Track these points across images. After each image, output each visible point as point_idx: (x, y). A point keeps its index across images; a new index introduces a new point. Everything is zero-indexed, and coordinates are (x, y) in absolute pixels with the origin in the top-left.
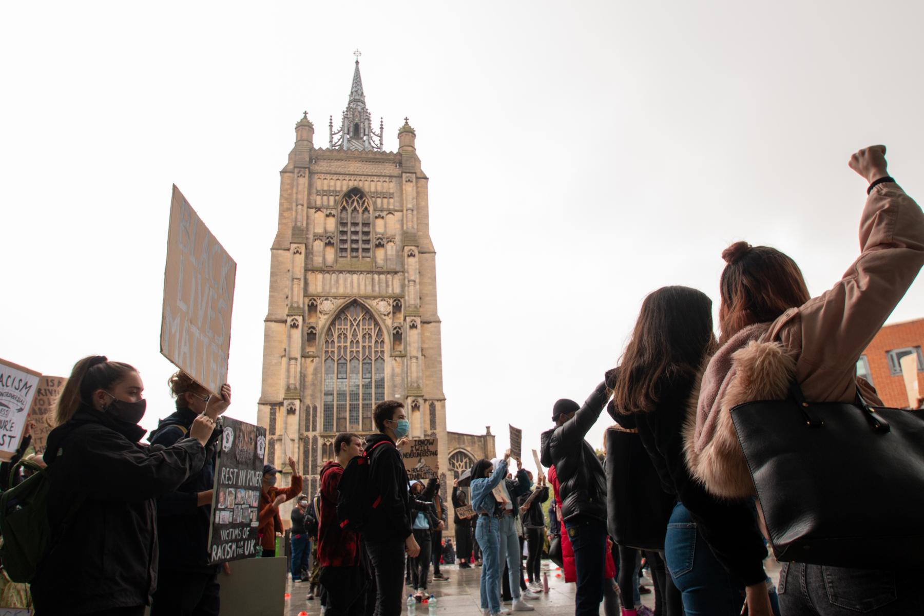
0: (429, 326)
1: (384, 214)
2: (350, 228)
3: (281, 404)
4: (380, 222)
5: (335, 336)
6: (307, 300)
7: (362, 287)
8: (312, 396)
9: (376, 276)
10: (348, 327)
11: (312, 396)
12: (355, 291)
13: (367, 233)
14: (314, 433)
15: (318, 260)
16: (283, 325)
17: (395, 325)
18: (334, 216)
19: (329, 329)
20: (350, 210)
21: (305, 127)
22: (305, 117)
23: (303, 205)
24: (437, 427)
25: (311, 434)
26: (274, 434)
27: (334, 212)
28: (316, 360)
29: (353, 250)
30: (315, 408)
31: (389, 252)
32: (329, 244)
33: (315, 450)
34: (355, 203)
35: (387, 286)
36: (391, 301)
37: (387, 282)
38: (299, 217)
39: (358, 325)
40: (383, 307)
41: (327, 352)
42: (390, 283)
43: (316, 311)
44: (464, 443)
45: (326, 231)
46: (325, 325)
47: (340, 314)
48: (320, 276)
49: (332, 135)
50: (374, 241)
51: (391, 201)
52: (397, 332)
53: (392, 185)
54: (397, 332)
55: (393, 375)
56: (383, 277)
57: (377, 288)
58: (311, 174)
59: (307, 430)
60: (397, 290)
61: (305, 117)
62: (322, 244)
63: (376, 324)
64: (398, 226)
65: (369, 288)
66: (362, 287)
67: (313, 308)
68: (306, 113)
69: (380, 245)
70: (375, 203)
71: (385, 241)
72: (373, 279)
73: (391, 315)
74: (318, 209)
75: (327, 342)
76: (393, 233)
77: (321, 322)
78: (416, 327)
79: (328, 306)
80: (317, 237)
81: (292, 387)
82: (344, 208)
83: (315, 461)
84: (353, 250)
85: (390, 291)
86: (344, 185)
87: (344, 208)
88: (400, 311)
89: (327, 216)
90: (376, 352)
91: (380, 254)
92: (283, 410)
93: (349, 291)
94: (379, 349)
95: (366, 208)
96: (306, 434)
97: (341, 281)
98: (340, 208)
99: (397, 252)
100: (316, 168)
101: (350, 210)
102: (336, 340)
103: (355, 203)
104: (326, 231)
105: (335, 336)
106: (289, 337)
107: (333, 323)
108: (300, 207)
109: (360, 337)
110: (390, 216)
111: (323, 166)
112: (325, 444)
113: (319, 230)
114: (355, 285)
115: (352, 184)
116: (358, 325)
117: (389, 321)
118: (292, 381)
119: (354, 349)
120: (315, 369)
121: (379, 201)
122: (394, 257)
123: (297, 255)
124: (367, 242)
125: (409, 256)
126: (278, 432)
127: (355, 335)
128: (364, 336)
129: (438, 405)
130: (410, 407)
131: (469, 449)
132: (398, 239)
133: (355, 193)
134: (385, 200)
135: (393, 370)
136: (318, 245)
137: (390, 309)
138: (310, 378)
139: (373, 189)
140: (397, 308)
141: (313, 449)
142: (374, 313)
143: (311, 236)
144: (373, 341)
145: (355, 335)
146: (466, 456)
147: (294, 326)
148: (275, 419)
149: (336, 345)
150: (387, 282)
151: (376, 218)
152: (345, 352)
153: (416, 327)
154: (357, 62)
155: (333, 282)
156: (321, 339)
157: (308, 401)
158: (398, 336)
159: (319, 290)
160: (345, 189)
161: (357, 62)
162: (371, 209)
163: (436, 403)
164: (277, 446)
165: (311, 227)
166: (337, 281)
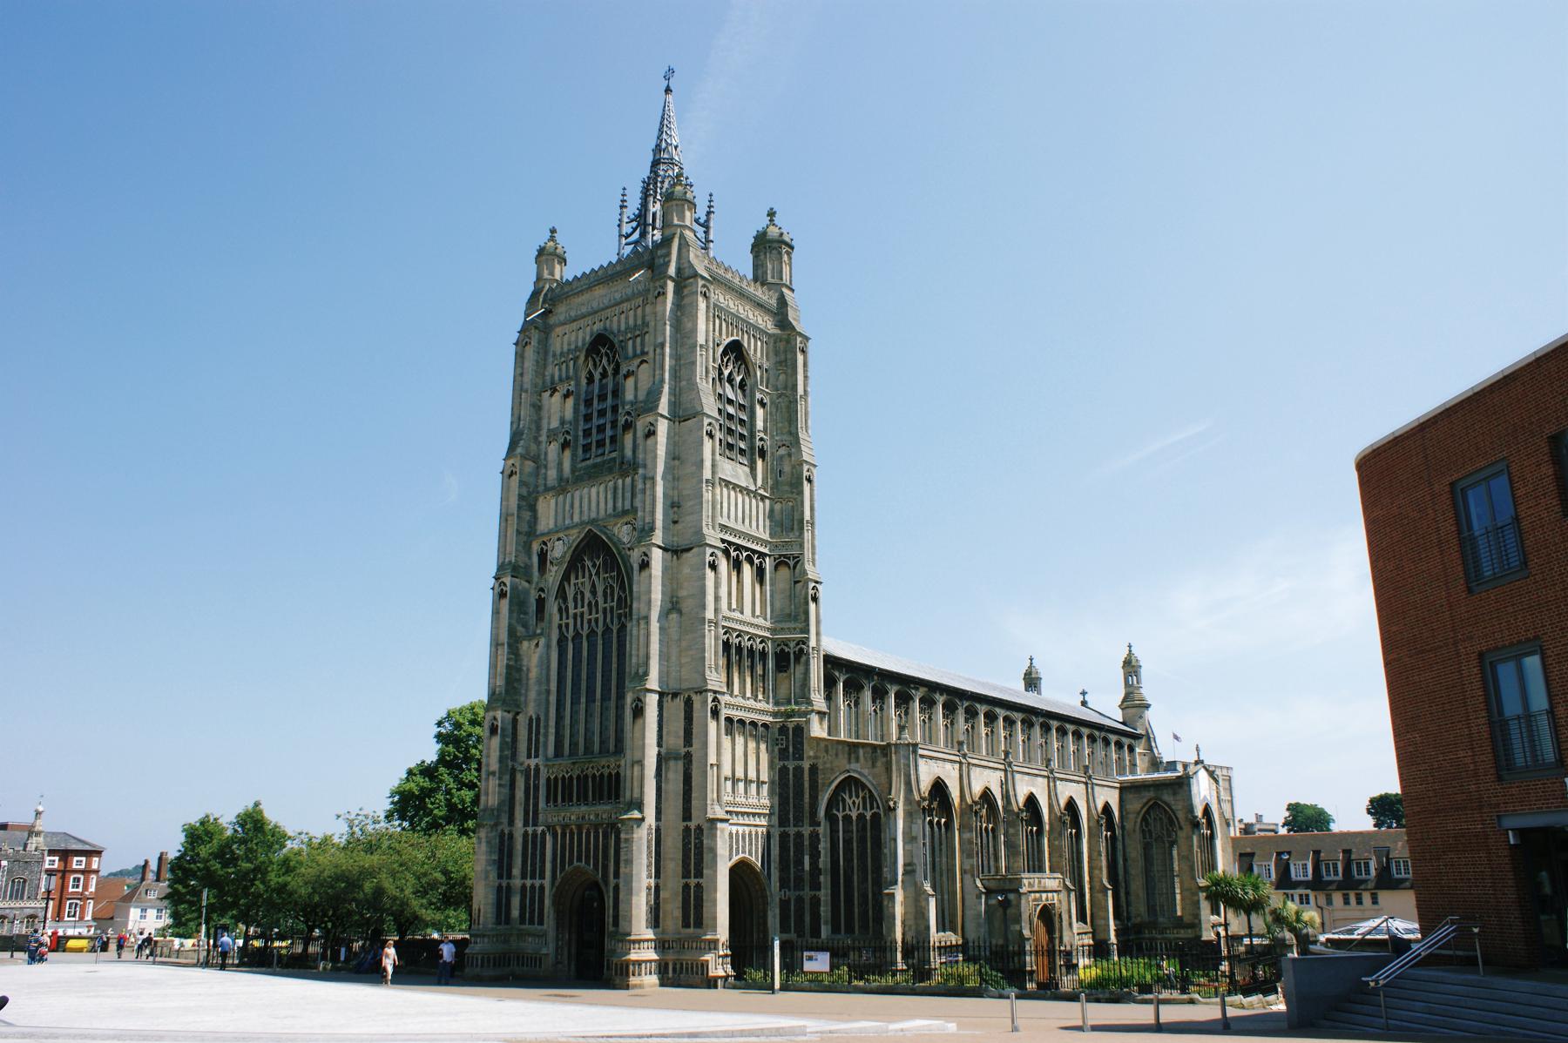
4: (630, 382)
6: (536, 547)
7: (602, 505)
13: (615, 409)
20: (597, 376)
22: (552, 239)
25: (533, 762)
28: (542, 641)
30: (538, 719)
33: (537, 788)
34: (604, 361)
39: (598, 574)
40: (623, 533)
41: (560, 627)
44: (857, 760)
47: (574, 564)
50: (622, 420)
57: (619, 504)
59: (529, 757)
66: (602, 505)
68: (553, 231)
69: (628, 426)
70: (624, 348)
72: (615, 489)
74: (554, 390)
75: (560, 610)
79: (558, 550)
80: (552, 435)
83: (536, 805)
84: (600, 444)
86: (580, 335)
89: (566, 396)
96: (528, 762)
98: (583, 375)
100: (552, 320)
101: (597, 376)
102: (571, 605)
103: (604, 361)
104: (563, 422)
107: (566, 577)
111: (562, 311)
112: (548, 779)
115: (598, 327)
119: (594, 616)
120: (541, 657)
124: (614, 424)
127: (594, 592)
129: (696, 699)
131: (866, 772)
133: (601, 344)
138: (534, 674)
143: (543, 438)
145: (594, 592)
146: (864, 787)
149: (571, 611)
151: (626, 377)
154: (668, 90)
156: (552, 607)
157: (531, 710)
163: (694, 697)
165: (545, 422)
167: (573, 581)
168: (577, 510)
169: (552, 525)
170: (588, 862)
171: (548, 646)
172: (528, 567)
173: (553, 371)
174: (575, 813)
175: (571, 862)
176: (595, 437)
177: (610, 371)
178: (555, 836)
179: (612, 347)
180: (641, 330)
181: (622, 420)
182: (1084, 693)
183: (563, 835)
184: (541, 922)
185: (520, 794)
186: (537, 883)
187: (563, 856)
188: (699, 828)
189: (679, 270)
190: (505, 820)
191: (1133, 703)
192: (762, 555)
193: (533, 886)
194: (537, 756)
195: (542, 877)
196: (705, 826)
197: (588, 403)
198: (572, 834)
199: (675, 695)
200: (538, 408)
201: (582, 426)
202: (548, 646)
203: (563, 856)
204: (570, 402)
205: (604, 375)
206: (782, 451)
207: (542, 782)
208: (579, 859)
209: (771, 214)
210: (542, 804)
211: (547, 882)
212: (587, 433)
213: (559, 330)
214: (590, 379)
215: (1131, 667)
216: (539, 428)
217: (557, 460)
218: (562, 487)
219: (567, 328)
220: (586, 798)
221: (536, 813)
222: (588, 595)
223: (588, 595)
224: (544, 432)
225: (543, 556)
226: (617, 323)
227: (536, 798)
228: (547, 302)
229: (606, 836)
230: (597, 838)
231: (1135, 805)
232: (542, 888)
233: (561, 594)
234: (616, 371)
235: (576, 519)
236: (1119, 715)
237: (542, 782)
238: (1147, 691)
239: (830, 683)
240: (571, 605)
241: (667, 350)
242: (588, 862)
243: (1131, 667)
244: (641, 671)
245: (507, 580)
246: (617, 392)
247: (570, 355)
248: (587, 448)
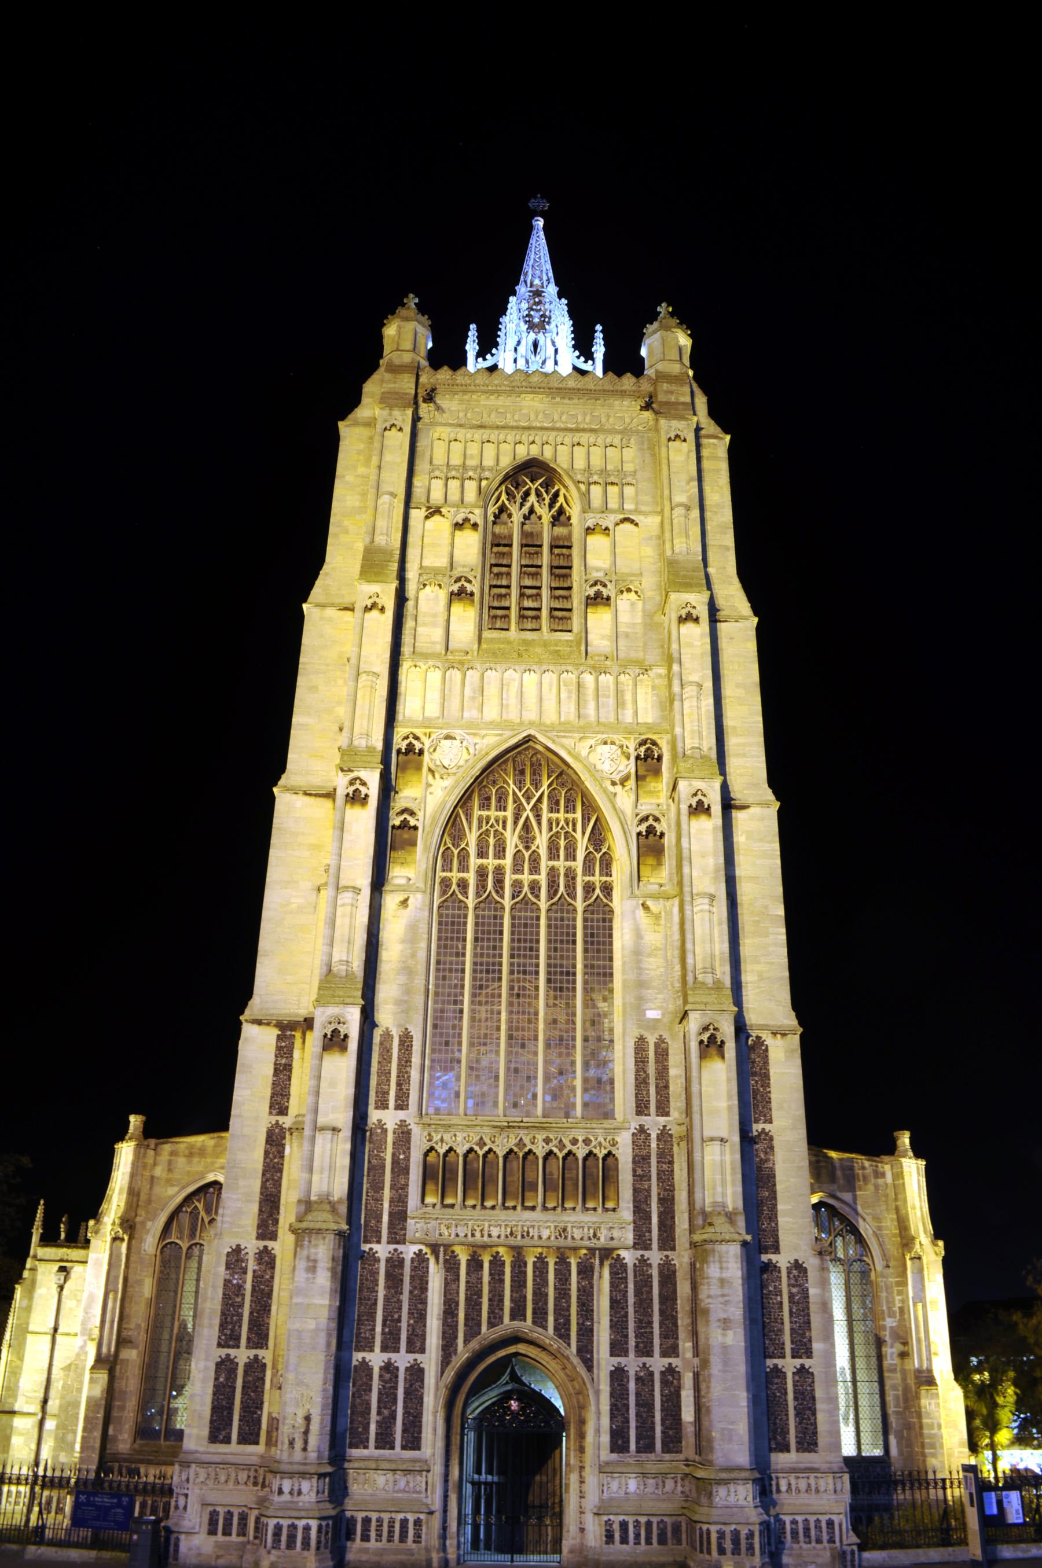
3: (308, 1023)
5: (472, 838)
7: (550, 705)
8: (398, 1002)
9: (589, 679)
10: (509, 814)
11: (398, 1002)
12: (531, 715)
14: (401, 1115)
16: (328, 803)
17: (644, 810)
18: (475, 526)
23: (393, 495)
24: (775, 1114)
26: (283, 1111)
27: (477, 517)
31: (624, 618)
32: (460, 595)
35: (620, 703)
36: (632, 745)
37: (619, 693)
38: (381, 524)
39: (536, 810)
42: (628, 697)
43: (419, 767)
46: (444, 803)
51: (629, 491)
52: (651, 830)
53: (629, 454)
54: (651, 830)
55: (637, 953)
57: (590, 710)
60: (648, 714)
62: (443, 595)
63: (590, 807)
64: (649, 551)
65: (569, 709)
66: (550, 705)
69: (598, 600)
71: (609, 591)
73: (631, 783)
76: (635, 567)
78: (707, 811)
81: (339, 969)
85: (628, 716)
87: (502, 509)
88: (657, 772)
89: (458, 526)
90: (589, 888)
91: (599, 620)
92: (315, 1038)
93: (513, 715)
94: (597, 879)
95: (561, 511)
97: (492, 690)
99: (648, 615)
101: (517, 516)
103: (532, 498)
105: (472, 838)
106: (341, 827)
107: (464, 800)
108: (386, 498)
109: (541, 842)
110: (627, 526)
113: (437, 560)
116: (536, 810)
117: (625, 799)
118: (339, 954)
122: (640, 630)
123: (375, 613)
125: (682, 620)
126: (295, 1106)
127: (527, 837)
130: (694, 1046)
132: (649, 583)
133: (532, 473)
134: (613, 490)
135: (638, 935)
140: (648, 761)
141: (395, 1162)
142: (584, 776)
144: (580, 854)
145: (527, 837)
147: (356, 799)
148: (288, 1067)
150: (619, 693)
151: (589, 531)
152: (499, 882)
153: (707, 811)
155: (468, 692)
158: (650, 843)
159: (433, 710)
162: (574, 511)
164: (293, 1151)
167: (477, 813)
168: (513, 700)
169: (433, 710)
170: (540, 1318)
174: (494, 1224)
175: (495, 1319)
178: (451, 1266)
183: (475, 1264)
184: (413, 1441)
186: (402, 1360)
187: (474, 1303)
188: (798, 1266)
193: (389, 1368)
194: (401, 1106)
195: (417, 1343)
196: (812, 1263)
198: (497, 1263)
203: (474, 1303)
208: (518, 1312)
211: (430, 1360)
213: (439, 429)
223: (512, 840)
229: (586, 1271)
230: (563, 1277)
232: (416, 1373)
233: (453, 827)
235: (491, 712)
242: (540, 1318)
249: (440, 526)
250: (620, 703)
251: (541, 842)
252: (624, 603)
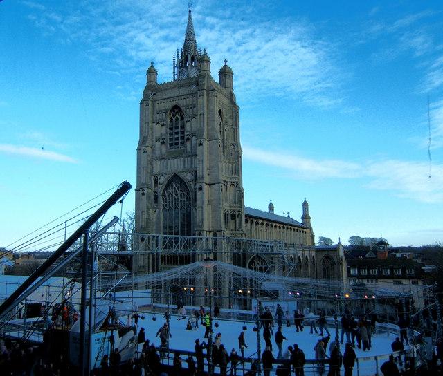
0: (214, 186)
1: (190, 119)
2: (175, 131)
4: (188, 124)
6: (153, 177)
13: (183, 132)
15: (158, 153)
19: (164, 192)
20: (174, 119)
21: (152, 72)
22: (152, 66)
29: (177, 144)
32: (163, 143)
33: (157, 259)
40: (188, 177)
41: (163, 205)
45: (162, 135)
47: (169, 184)
48: (159, 163)
49: (174, 67)
50: (186, 137)
56: (189, 158)
57: (186, 166)
58: (154, 101)
61: (152, 66)
63: (186, 187)
67: (156, 181)
72: (184, 161)
74: (157, 123)
77: (160, 188)
79: (162, 180)
80: (157, 140)
82: (171, 118)
83: (157, 264)
84: (177, 144)
86: (169, 105)
87: (171, 118)
89: (163, 125)
91: (188, 144)
100: (156, 97)
101: (174, 119)
102: (168, 198)
104: (162, 135)
107: (166, 189)
109: (179, 195)
111: (159, 95)
113: (158, 135)
114: (176, 165)
115: (174, 103)
121: (188, 110)
124: (183, 138)
127: (176, 195)
128: (181, 195)
133: (176, 108)
136: (158, 144)
137: (193, 178)
139: (185, 104)
143: (154, 140)
145: (176, 195)
147: (143, 194)
149: (168, 200)
150: (191, 161)
154: (190, 11)
156: (160, 199)
160: (171, 106)
161: (190, 11)
165: (154, 134)
166: (167, 164)
168: (172, 166)
171: (159, 211)
172: (151, 185)
173: (158, 117)
176: (174, 141)
177: (179, 118)
179: (180, 109)
180: (193, 106)
181: (186, 137)
182: (289, 213)
185: (151, 261)
189: (208, 87)
190: (147, 270)
191: (306, 217)
192: (227, 182)
197: (171, 129)
199: (210, 232)
200: (152, 129)
201: (168, 137)
202: (159, 211)
204: (164, 128)
205: (177, 119)
206: (232, 147)
207: (159, 257)
209: (226, 61)
210: (159, 264)
212: (171, 139)
214: (171, 120)
215: (305, 205)
216: (152, 136)
217: (161, 149)
218: (163, 158)
219: (162, 101)
220: (171, 262)
221: (157, 267)
222: (174, 196)
223: (174, 196)
224: (154, 137)
225: (156, 181)
226: (182, 103)
227: (157, 262)
228: (153, 90)
231: (321, 256)
234: (182, 118)
236: (300, 221)
237: (159, 257)
238: (310, 213)
239: (247, 221)
240: (168, 198)
241: (205, 116)
243: (305, 205)
244: (201, 224)
245: (146, 189)
246: (183, 127)
247: (165, 111)
248: (171, 145)
249: (159, 125)
250: (192, 164)
251: (179, 195)
252: (193, 139)
